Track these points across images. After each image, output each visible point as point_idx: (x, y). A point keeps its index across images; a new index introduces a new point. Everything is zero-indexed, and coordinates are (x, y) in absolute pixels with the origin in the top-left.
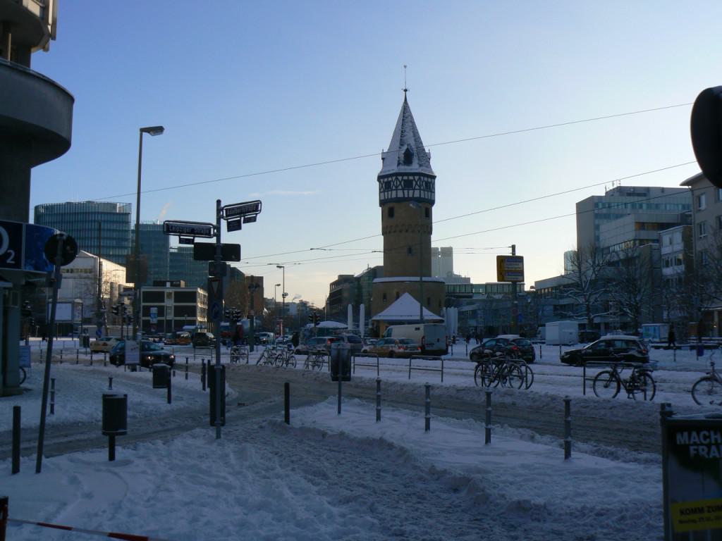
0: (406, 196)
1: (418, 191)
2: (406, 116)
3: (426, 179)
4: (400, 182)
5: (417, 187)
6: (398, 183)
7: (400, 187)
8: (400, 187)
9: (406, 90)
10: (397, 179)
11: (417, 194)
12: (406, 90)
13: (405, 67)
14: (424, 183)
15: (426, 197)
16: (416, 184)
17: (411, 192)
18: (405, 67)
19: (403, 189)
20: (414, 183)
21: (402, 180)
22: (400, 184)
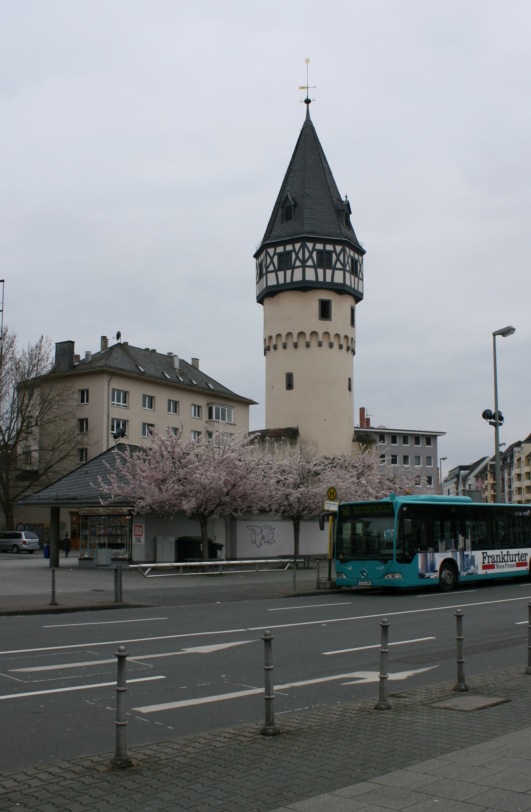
0: (281, 281)
1: (301, 269)
2: (308, 143)
3: (320, 246)
4: (272, 259)
5: (298, 263)
6: (269, 260)
7: (271, 268)
8: (271, 268)
9: (308, 101)
10: (267, 253)
11: (298, 276)
12: (308, 101)
13: (307, 61)
14: (314, 255)
15: (321, 279)
16: (297, 257)
17: (289, 272)
18: (307, 61)
19: (275, 271)
20: (294, 256)
21: (275, 253)
22: (272, 262)
